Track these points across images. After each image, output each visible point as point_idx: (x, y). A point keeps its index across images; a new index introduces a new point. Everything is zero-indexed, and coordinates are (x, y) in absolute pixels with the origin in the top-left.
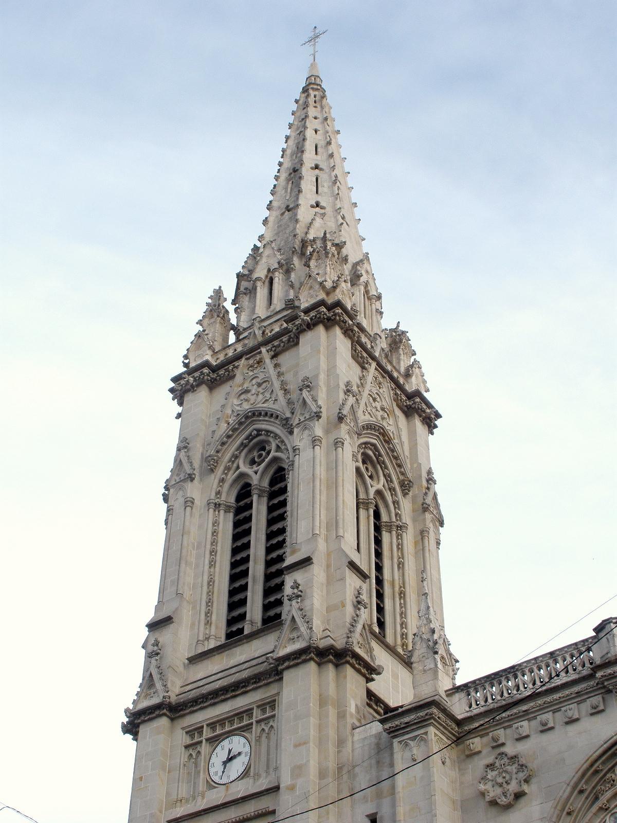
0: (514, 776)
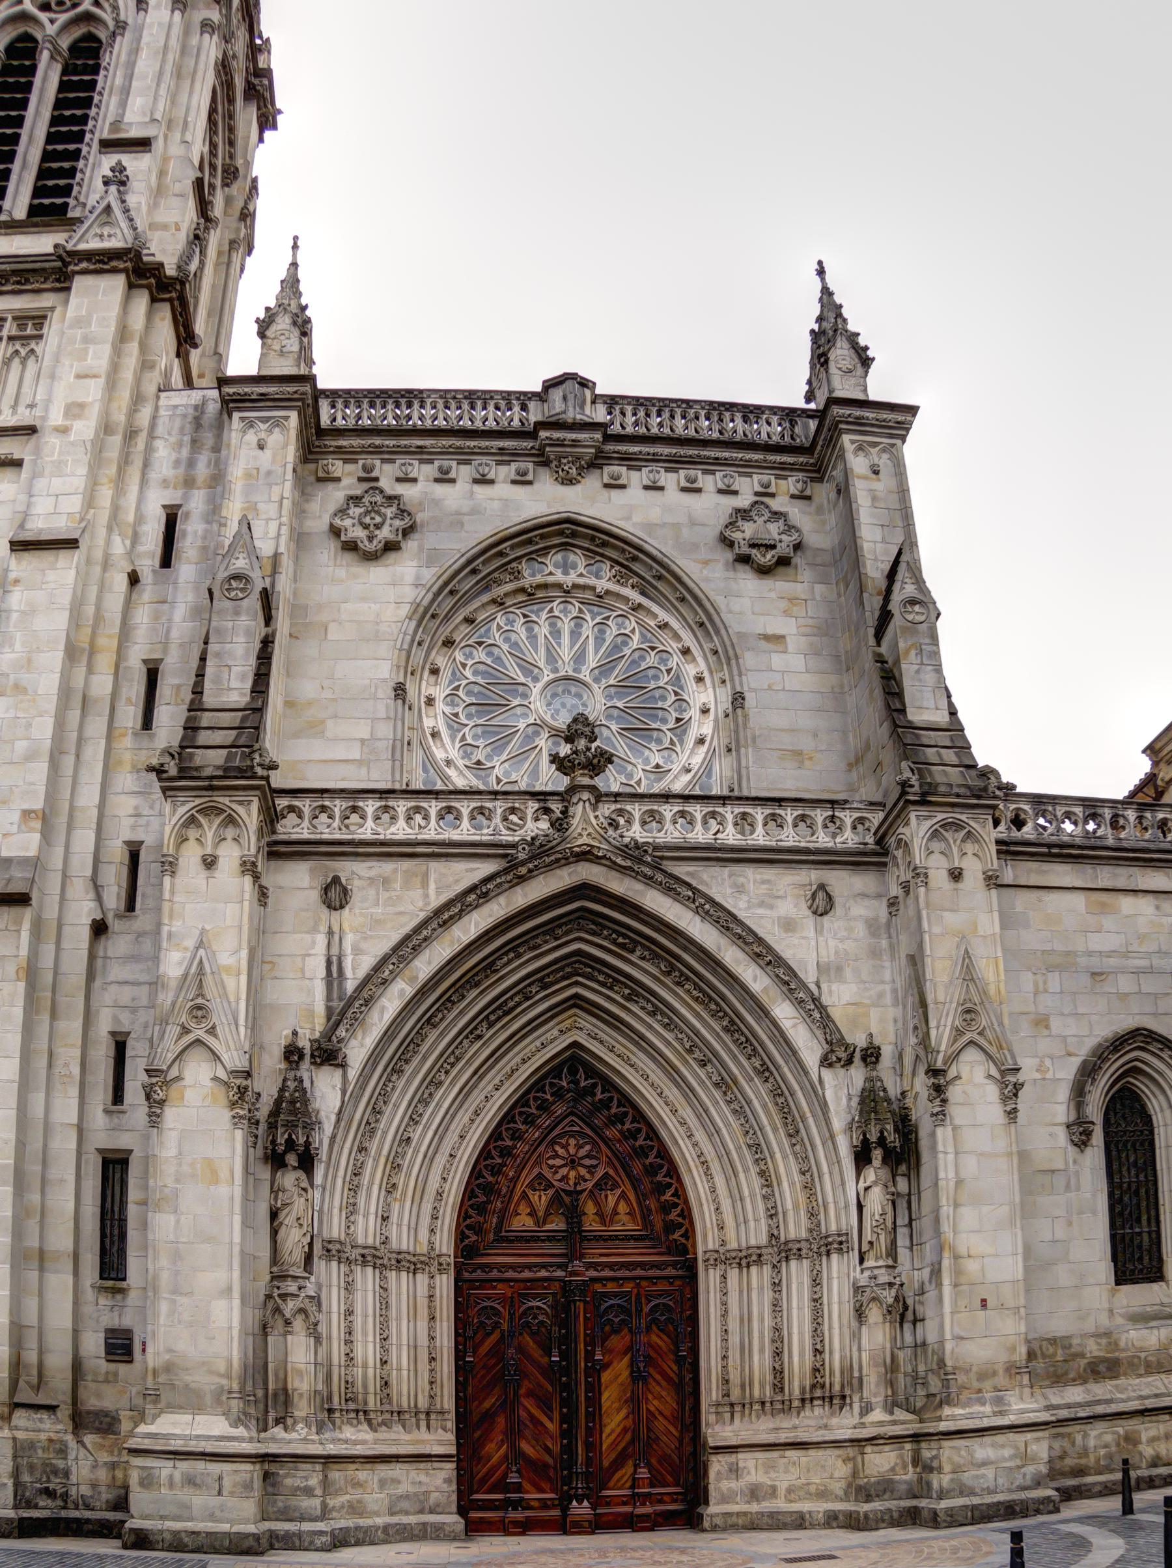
0: (388, 521)
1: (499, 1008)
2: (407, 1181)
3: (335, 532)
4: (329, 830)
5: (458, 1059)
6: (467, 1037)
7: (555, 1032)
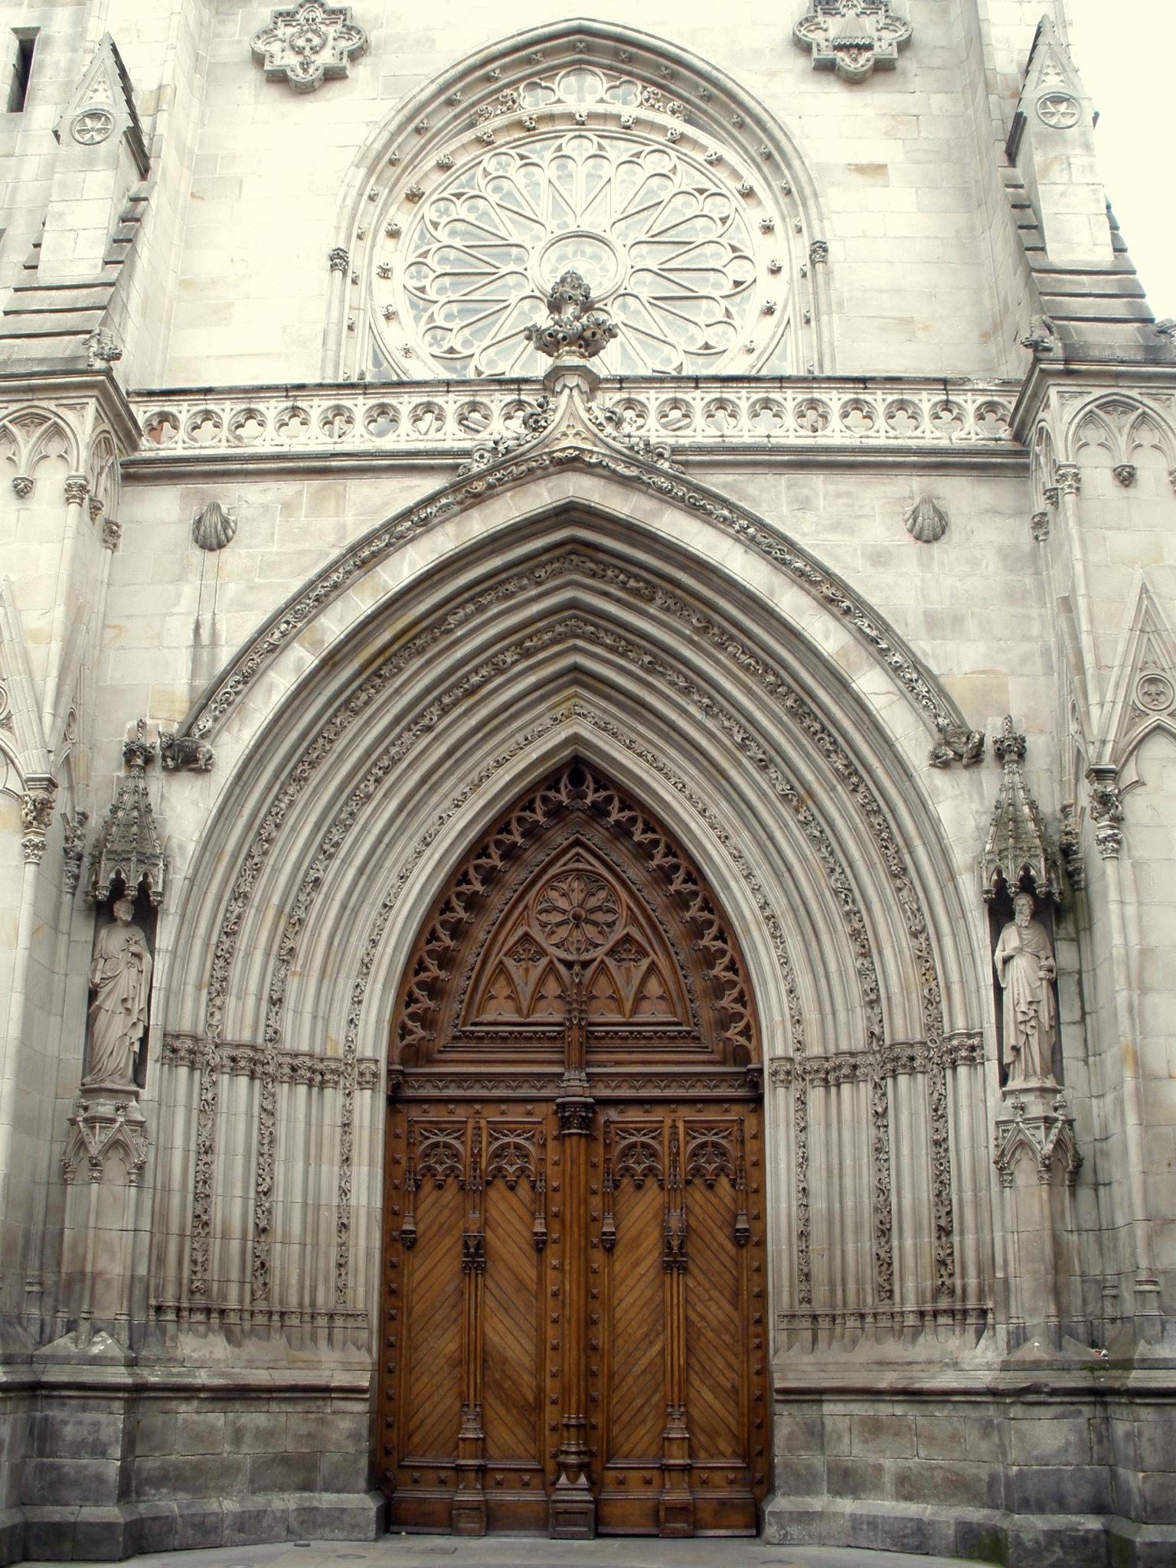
0: (331, 42)
1: (457, 685)
2: (313, 946)
3: (258, 59)
4: (212, 442)
5: (395, 762)
7: (547, 721)
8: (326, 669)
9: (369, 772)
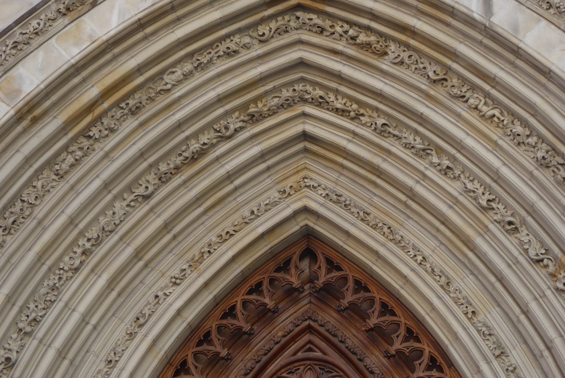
6: (119, 196)
8: (25, 123)
9: (75, 242)
